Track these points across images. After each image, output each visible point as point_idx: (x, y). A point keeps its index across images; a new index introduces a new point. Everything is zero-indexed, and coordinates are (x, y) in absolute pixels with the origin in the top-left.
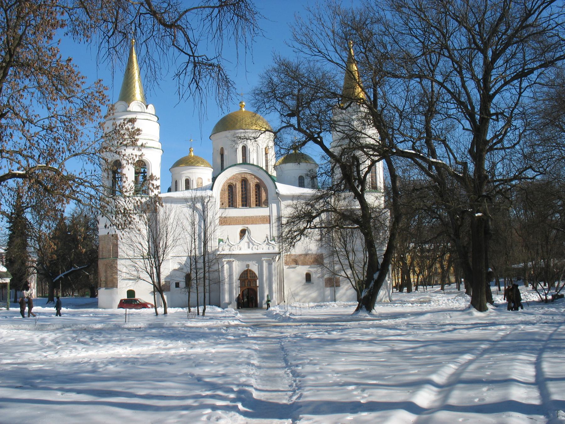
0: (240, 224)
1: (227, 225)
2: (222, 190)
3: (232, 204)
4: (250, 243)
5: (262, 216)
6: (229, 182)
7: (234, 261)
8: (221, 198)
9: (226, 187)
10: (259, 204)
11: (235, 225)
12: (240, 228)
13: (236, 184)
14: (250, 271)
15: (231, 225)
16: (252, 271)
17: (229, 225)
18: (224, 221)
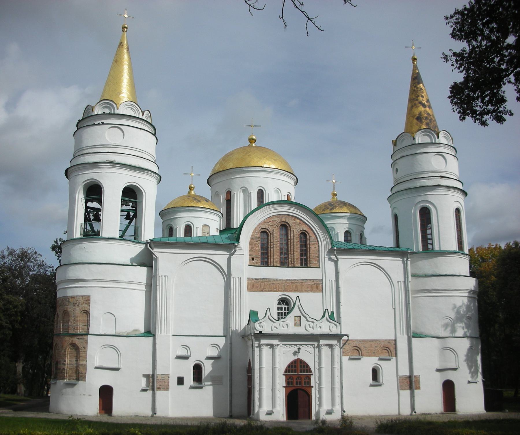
0: (279, 291)
1: (260, 291)
2: (252, 239)
3: (265, 262)
4: (302, 317)
5: (310, 280)
6: (263, 227)
7: (278, 345)
8: (250, 250)
9: (258, 235)
10: (305, 263)
11: (271, 291)
12: (277, 296)
13: (273, 231)
14: (301, 361)
15: (266, 291)
16: (304, 362)
17: (262, 291)
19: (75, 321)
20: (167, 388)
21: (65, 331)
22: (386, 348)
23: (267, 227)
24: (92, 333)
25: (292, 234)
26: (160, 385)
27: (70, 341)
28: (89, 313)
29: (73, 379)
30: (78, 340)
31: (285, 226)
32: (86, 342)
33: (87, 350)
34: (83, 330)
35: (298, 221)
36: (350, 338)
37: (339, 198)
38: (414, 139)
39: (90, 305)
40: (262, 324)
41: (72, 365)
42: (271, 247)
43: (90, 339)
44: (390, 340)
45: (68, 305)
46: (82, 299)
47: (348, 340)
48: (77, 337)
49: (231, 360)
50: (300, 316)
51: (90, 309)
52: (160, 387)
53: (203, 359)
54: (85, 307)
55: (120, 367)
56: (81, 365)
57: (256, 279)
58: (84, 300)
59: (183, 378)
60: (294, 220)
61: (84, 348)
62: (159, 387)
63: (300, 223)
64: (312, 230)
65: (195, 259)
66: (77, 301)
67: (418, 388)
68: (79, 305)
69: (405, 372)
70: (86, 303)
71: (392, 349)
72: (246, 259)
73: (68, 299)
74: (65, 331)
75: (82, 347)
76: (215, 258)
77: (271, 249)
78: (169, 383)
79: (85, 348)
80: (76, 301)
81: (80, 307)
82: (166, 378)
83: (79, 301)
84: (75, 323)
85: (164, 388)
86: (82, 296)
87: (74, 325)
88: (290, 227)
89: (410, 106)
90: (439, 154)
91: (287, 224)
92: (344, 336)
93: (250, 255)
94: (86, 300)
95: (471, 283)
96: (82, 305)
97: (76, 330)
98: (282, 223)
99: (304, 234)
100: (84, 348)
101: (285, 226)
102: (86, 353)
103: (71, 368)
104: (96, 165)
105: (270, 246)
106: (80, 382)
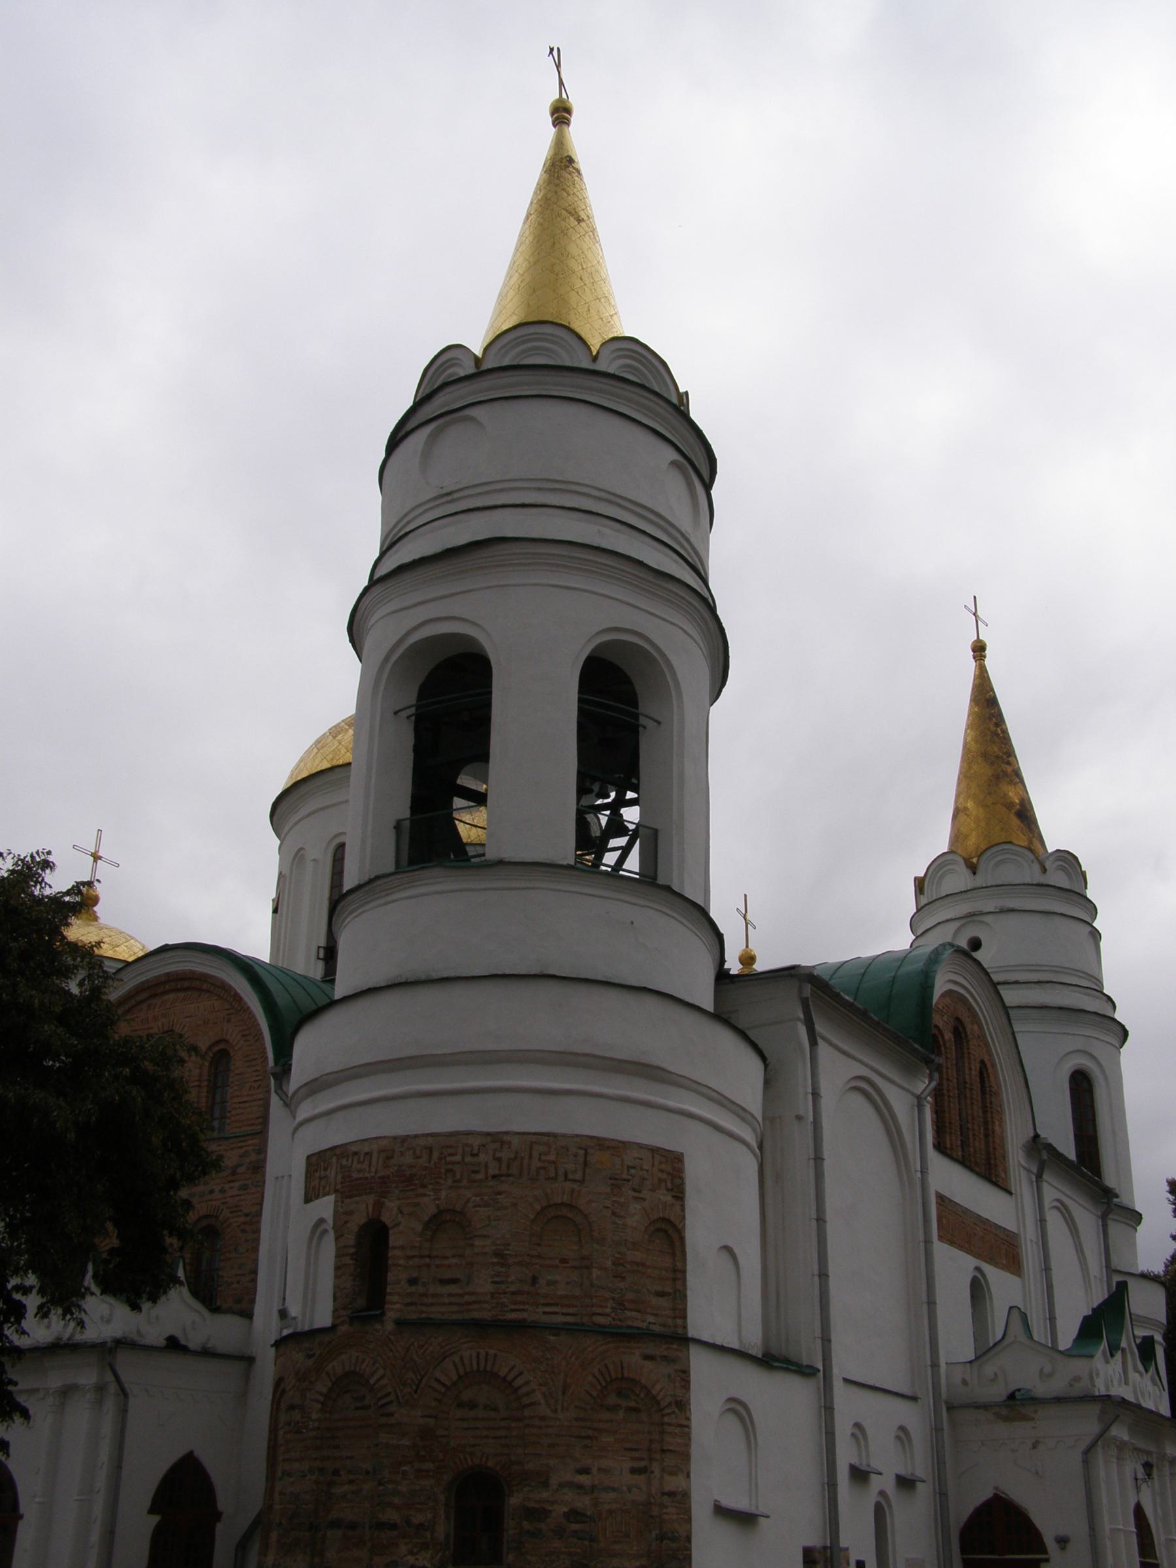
19: (622, 1265)
21: (547, 1309)
25: (973, 1067)
27: (606, 1366)
30: (649, 1365)
32: (684, 1376)
33: (688, 1419)
34: (656, 1315)
35: (976, 1027)
41: (613, 1495)
42: (949, 1096)
45: (582, 1182)
46: (653, 1165)
51: (684, 1218)
56: (671, 1494)
58: (662, 1171)
66: (633, 1171)
68: (640, 1192)
70: (669, 1185)
73: (582, 1152)
74: (547, 1309)
75: (670, 1404)
77: (949, 1102)
79: (682, 1405)
80: (629, 1167)
81: (644, 1199)
83: (642, 1169)
84: (624, 1278)
86: (654, 1150)
87: (622, 1285)
88: (968, 1041)
91: (961, 1029)
94: (669, 1174)
96: (653, 1190)
97: (631, 1310)
103: (610, 1511)
104: (663, 584)
105: (949, 1091)
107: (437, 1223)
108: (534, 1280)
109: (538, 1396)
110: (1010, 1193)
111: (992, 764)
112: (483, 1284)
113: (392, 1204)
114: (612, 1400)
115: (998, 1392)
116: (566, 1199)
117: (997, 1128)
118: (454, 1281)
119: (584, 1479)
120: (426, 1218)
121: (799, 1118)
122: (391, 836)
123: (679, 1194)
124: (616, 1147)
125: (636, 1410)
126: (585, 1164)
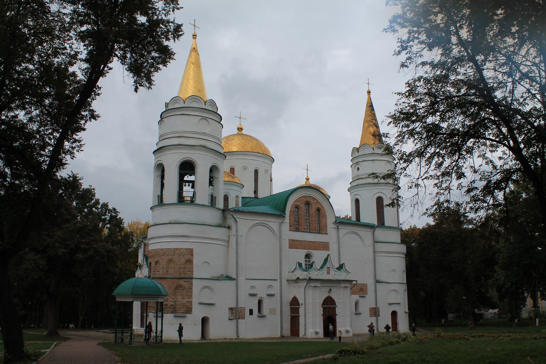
4: (331, 269)
5: (323, 242)
8: (290, 220)
11: (301, 249)
12: (304, 252)
15: (299, 249)
17: (297, 248)
18: (294, 244)
20: (244, 318)
22: (361, 290)
23: (298, 204)
24: (196, 277)
26: (240, 316)
28: (192, 261)
29: (180, 313)
30: (185, 283)
31: (308, 204)
35: (316, 201)
36: (358, 282)
37: (312, 182)
38: (373, 150)
39: (193, 256)
40: (310, 272)
43: (194, 281)
44: (364, 284)
47: (357, 284)
48: (185, 280)
49: (281, 297)
50: (329, 268)
52: (240, 317)
53: (264, 296)
54: (189, 257)
55: (214, 303)
56: (188, 302)
57: (293, 240)
59: (252, 309)
60: (314, 200)
61: (190, 288)
62: (239, 317)
63: (317, 203)
64: (323, 207)
65: (257, 225)
67: (379, 316)
69: (373, 306)
71: (365, 290)
72: (288, 225)
76: (270, 224)
78: (245, 313)
79: (191, 288)
82: (243, 310)
85: (242, 318)
86: (187, 249)
89: (366, 125)
90: (389, 162)
92: (354, 282)
93: (290, 223)
95: (403, 248)
98: (306, 202)
99: (318, 210)
100: (190, 288)
101: (308, 204)
102: (191, 292)
106: (188, 315)
107: (157, 262)
108: (167, 271)
109: (166, 288)
110: (327, 234)
111: (368, 123)
112: (161, 272)
113: (152, 260)
114: (179, 288)
115: (295, 278)
116: (171, 258)
117: (324, 220)
118: (158, 271)
119: (173, 300)
120: (155, 262)
121: (234, 235)
122: (157, 198)
123: (192, 255)
124: (180, 249)
125: (183, 289)
126: (174, 252)
